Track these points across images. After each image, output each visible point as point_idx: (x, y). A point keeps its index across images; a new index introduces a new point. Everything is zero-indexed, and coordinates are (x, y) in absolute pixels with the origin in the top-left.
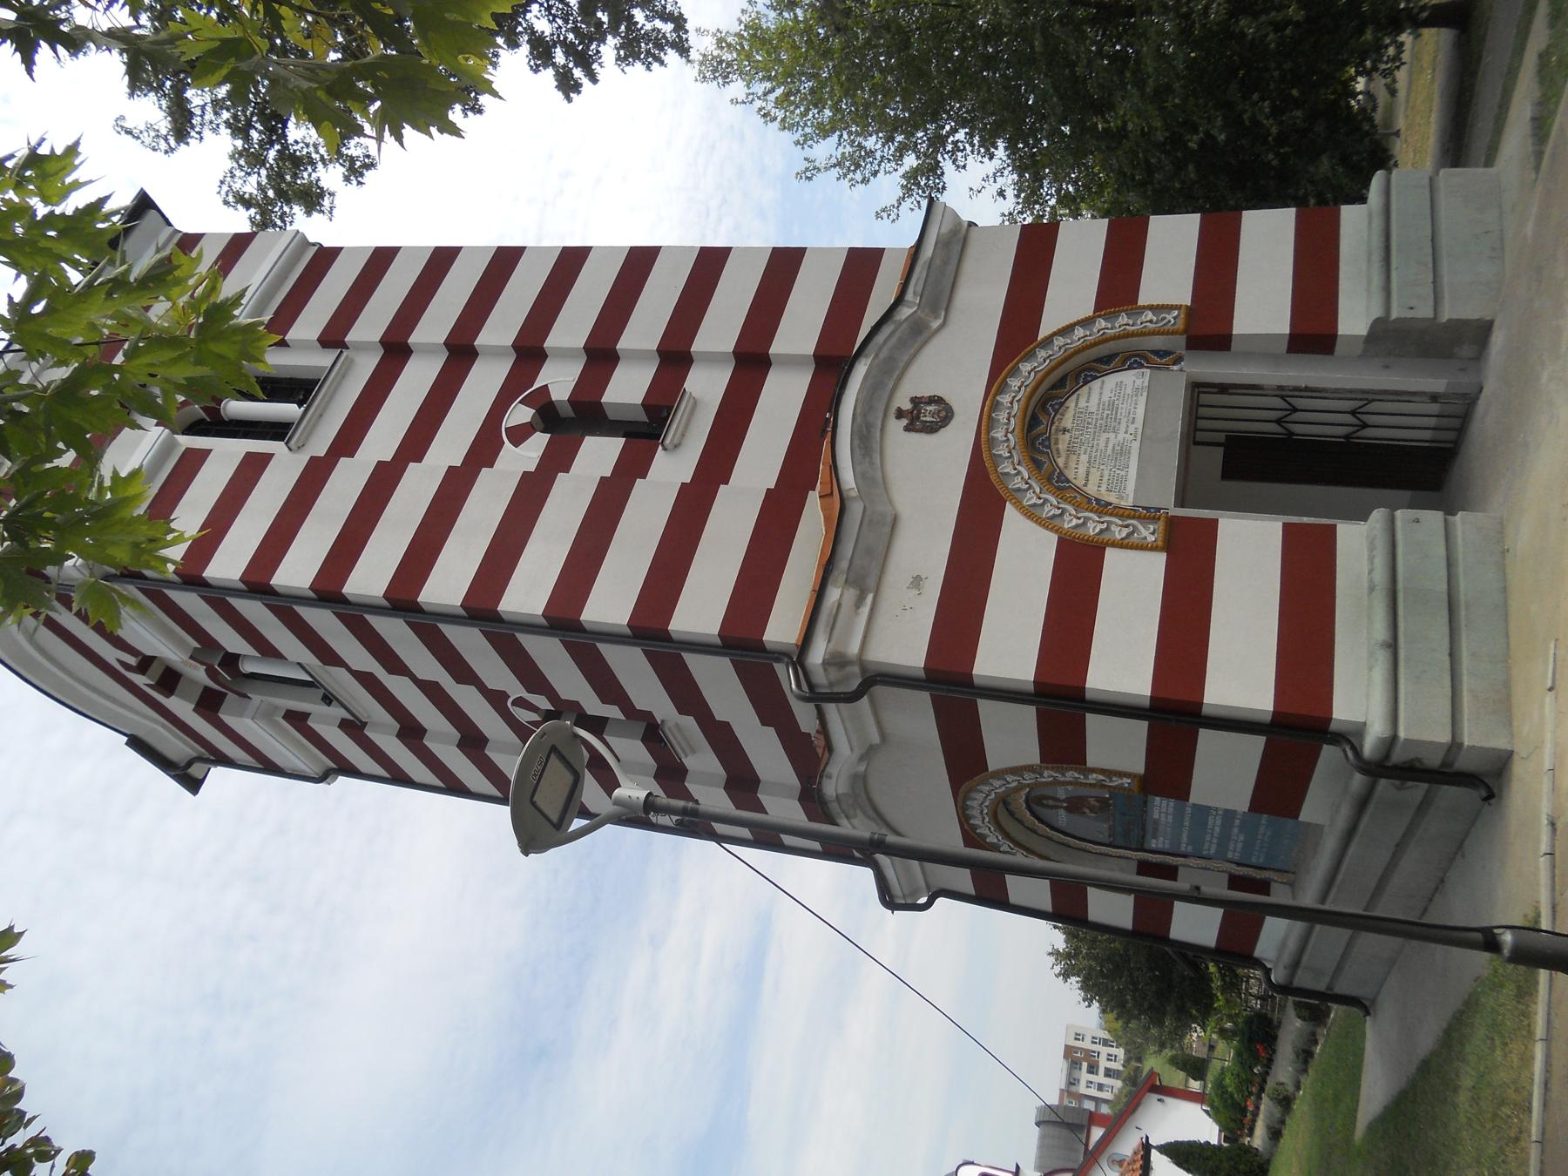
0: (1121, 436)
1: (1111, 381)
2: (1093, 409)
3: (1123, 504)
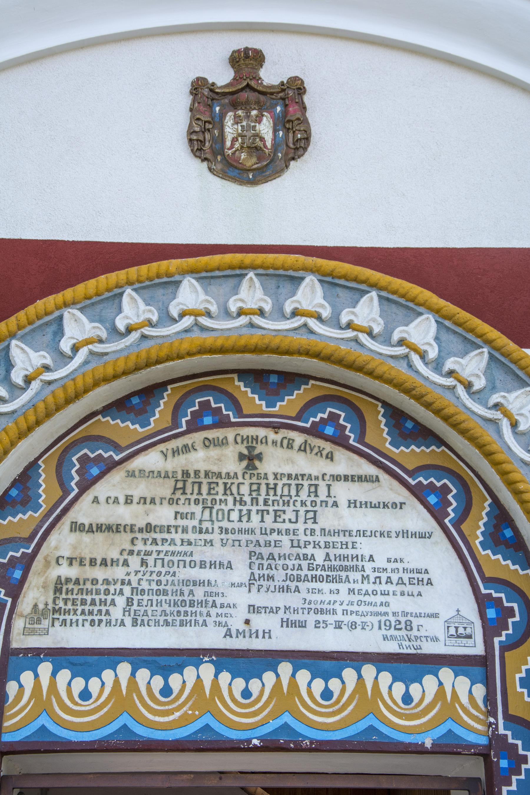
0: (242, 598)
1: (438, 558)
2: (328, 519)
3: (18, 624)
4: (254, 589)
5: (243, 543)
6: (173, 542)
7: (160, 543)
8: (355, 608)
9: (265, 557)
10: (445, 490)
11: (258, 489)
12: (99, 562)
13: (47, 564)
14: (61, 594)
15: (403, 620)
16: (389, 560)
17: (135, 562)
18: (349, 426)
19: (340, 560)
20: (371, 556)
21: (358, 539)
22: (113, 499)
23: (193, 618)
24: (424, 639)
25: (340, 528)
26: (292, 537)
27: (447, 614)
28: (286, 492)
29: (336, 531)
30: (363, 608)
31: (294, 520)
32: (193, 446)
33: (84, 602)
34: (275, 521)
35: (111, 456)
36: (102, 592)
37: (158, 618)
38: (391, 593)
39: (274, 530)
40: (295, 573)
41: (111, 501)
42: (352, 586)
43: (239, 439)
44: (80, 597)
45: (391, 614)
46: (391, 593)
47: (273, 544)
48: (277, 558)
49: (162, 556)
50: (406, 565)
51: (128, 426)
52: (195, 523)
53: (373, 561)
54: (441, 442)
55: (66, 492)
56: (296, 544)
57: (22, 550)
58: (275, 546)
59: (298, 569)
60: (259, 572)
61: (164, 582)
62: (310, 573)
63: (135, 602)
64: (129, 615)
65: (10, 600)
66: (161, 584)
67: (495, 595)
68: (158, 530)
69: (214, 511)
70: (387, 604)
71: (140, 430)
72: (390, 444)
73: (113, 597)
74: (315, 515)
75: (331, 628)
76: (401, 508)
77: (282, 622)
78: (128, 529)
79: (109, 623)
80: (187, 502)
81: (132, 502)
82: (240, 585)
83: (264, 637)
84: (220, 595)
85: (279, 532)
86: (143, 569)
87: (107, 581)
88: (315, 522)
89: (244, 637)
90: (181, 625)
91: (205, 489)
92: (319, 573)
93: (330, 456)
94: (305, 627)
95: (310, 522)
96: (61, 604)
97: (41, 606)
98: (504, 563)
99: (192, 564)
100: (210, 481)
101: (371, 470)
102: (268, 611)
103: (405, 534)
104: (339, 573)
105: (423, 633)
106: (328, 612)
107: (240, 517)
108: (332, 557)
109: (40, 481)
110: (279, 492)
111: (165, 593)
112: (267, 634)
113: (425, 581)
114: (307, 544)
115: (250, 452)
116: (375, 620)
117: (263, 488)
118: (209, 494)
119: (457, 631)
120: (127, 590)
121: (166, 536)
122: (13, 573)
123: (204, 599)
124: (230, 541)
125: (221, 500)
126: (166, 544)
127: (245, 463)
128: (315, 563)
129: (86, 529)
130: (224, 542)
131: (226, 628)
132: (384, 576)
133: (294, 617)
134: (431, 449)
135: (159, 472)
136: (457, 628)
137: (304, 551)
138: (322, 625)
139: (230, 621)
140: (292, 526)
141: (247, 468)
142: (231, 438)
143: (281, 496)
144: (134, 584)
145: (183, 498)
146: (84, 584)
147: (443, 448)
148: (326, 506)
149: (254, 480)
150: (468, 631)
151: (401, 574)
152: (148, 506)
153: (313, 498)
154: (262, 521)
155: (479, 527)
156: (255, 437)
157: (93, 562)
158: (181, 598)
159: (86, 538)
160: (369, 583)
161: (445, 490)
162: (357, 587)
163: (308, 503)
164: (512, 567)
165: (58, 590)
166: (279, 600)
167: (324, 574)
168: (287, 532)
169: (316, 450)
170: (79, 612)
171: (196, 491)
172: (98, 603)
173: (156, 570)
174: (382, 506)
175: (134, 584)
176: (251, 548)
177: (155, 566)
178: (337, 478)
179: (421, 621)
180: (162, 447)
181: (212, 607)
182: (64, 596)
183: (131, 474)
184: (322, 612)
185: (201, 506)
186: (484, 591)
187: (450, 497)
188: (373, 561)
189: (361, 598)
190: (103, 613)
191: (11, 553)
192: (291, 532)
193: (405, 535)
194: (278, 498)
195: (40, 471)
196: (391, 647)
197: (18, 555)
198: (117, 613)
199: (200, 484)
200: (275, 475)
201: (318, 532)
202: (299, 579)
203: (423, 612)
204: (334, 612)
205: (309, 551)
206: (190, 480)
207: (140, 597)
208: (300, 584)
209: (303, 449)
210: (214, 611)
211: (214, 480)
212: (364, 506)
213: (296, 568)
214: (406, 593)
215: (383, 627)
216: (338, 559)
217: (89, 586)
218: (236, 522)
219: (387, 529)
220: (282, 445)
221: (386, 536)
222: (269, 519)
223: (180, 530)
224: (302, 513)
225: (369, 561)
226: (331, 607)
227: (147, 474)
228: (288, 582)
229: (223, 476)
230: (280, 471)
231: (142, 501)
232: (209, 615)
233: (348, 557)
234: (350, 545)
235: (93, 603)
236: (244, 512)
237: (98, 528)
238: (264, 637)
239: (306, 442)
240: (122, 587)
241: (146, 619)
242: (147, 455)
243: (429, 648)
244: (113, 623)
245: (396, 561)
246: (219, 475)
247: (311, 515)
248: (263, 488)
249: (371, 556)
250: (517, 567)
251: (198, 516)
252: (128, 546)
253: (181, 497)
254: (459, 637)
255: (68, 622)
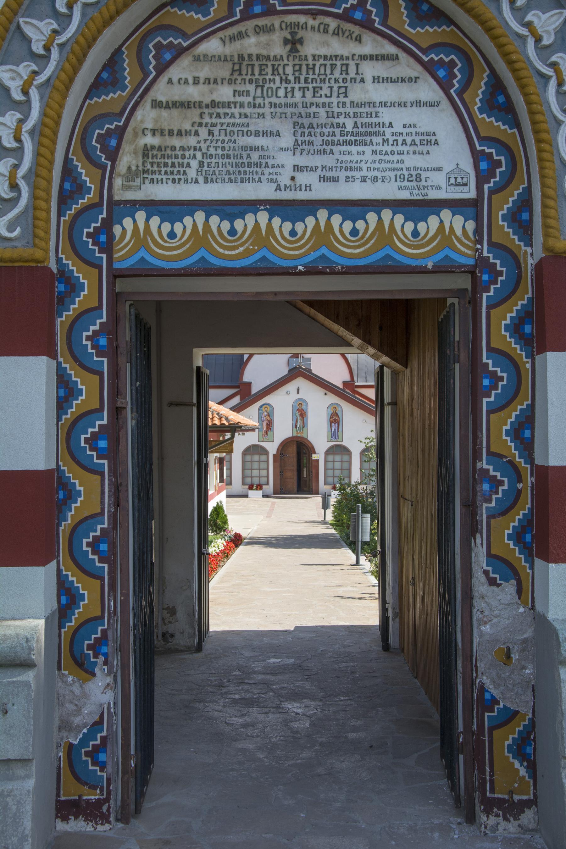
0: (288, 160)
1: (443, 124)
2: (356, 93)
3: (118, 182)
4: (298, 152)
5: (289, 115)
6: (233, 116)
7: (222, 116)
8: (377, 165)
9: (306, 126)
10: (452, 64)
11: (300, 70)
12: (175, 132)
13: (136, 135)
14: (148, 158)
15: (414, 173)
16: (404, 126)
17: (204, 132)
18: (374, 10)
19: (366, 127)
20: (390, 123)
21: (380, 110)
22: (183, 80)
23: (251, 176)
24: (430, 188)
25: (366, 101)
26: (328, 110)
27: (448, 167)
28: (322, 72)
29: (363, 103)
30: (383, 166)
31: (329, 95)
32: (246, 33)
33: (166, 165)
34: (314, 96)
35: (180, 43)
36: (180, 156)
37: (224, 176)
38: (405, 153)
39: (313, 104)
40: (330, 138)
41: (182, 82)
42: (374, 148)
43: (284, 26)
44: (163, 161)
45: (405, 170)
46: (405, 153)
47: (312, 115)
48: (316, 127)
49: (224, 127)
50: (418, 130)
51: (192, 15)
52: (250, 99)
53: (392, 127)
54: (451, 21)
55: (146, 74)
56: (330, 115)
57: (115, 123)
58: (314, 117)
59: (332, 136)
60: (301, 138)
61: (227, 148)
62: (341, 139)
63: (206, 165)
64: (202, 175)
65: (109, 163)
66: (225, 150)
67: (487, 151)
68: (220, 105)
69: (265, 89)
70: (402, 162)
71: (203, 19)
72: (408, 25)
73: (188, 161)
74: (346, 90)
75: (358, 182)
76: (416, 82)
77: (320, 178)
78: (197, 105)
79: (186, 181)
80: (243, 82)
81: (199, 82)
82: (287, 149)
83: (306, 190)
84: (272, 158)
85: (317, 106)
86: (210, 138)
87: (182, 148)
88: (346, 96)
89: (291, 190)
90: (242, 181)
91: (257, 72)
92: (349, 138)
93: (358, 38)
94: (338, 181)
95: (342, 96)
96: (149, 166)
97: (134, 168)
98: (496, 124)
99: (249, 134)
100: (261, 63)
101: (391, 49)
102: (309, 169)
103: (418, 103)
104: (365, 137)
105: (429, 183)
106: (355, 169)
107: (286, 93)
108: (359, 125)
109: (125, 65)
110: (317, 71)
111: (228, 157)
112: (308, 188)
113: (433, 142)
114: (339, 114)
115: (292, 37)
116: (392, 174)
117: (304, 68)
118: (260, 74)
119: (456, 181)
120: (199, 155)
121: (227, 110)
122: (110, 142)
123: (259, 161)
124: (278, 114)
125: (270, 79)
126: (228, 117)
127: (289, 47)
128: (346, 130)
129: (164, 105)
130: (274, 114)
131: (276, 184)
132: (400, 139)
133: (329, 174)
134: (442, 28)
135: (219, 56)
136: (456, 178)
137: (337, 120)
138: (351, 179)
139: (280, 178)
140: (327, 100)
141: (291, 51)
142: (277, 25)
143: (319, 75)
144: (204, 150)
145: (239, 78)
146: (165, 150)
147: (452, 27)
148: (355, 82)
149: (297, 62)
150: (465, 180)
151: (414, 137)
152: (212, 86)
153: (344, 76)
154: (304, 96)
155: (478, 96)
156: (297, 23)
157: (171, 133)
158: (241, 161)
159: (165, 113)
160: (388, 145)
161: (452, 64)
162: (378, 148)
163: (341, 80)
164: (502, 128)
165: (145, 155)
166: (318, 161)
167: (353, 139)
168: (324, 105)
169: (347, 34)
170: (163, 173)
171: (250, 72)
172: (177, 166)
173: (221, 138)
174: (400, 80)
175: (204, 150)
176: (295, 119)
177: (220, 135)
178: (364, 58)
179: (428, 174)
180: (221, 34)
181: (265, 167)
182: (150, 160)
183: (197, 59)
184: (351, 169)
185: (254, 85)
186: (479, 148)
187: (455, 71)
188: (392, 127)
189: (382, 157)
190: (182, 173)
191: (107, 126)
192: (327, 105)
193: (418, 104)
194: (316, 77)
195: (124, 56)
196: (405, 195)
197: (113, 127)
198: (192, 173)
199: (253, 66)
200: (314, 56)
201: (348, 105)
202: (333, 143)
203: (430, 166)
204: (361, 169)
205: (341, 120)
206: (245, 63)
207: (209, 160)
208: (333, 148)
209: (336, 33)
210: (266, 171)
211: (264, 62)
212: (385, 81)
213: (331, 135)
214: (417, 153)
215: (398, 179)
216: (364, 126)
217: (169, 152)
218: (282, 97)
219: (403, 100)
220: (319, 31)
221: (403, 105)
222: (309, 94)
223: (238, 105)
224: (335, 89)
225: (389, 127)
226: (358, 165)
227: (210, 59)
228: (324, 146)
229: (272, 58)
230: (318, 53)
231: (207, 82)
232: (263, 173)
233: (372, 125)
234: (374, 115)
235: (173, 165)
236: (289, 89)
237: (173, 105)
238: (306, 190)
239: (339, 26)
240: (194, 152)
241: (214, 177)
242: (209, 41)
243: (433, 195)
244: (190, 181)
245: (410, 126)
246: (268, 58)
247: (343, 90)
248: (304, 68)
249: (390, 123)
250: (506, 127)
251: (252, 93)
252: (197, 120)
253: (238, 77)
254: (457, 185)
255: (155, 180)
